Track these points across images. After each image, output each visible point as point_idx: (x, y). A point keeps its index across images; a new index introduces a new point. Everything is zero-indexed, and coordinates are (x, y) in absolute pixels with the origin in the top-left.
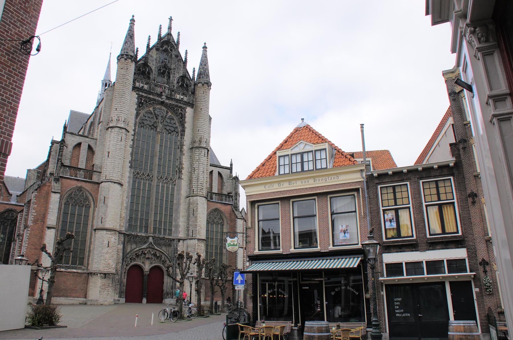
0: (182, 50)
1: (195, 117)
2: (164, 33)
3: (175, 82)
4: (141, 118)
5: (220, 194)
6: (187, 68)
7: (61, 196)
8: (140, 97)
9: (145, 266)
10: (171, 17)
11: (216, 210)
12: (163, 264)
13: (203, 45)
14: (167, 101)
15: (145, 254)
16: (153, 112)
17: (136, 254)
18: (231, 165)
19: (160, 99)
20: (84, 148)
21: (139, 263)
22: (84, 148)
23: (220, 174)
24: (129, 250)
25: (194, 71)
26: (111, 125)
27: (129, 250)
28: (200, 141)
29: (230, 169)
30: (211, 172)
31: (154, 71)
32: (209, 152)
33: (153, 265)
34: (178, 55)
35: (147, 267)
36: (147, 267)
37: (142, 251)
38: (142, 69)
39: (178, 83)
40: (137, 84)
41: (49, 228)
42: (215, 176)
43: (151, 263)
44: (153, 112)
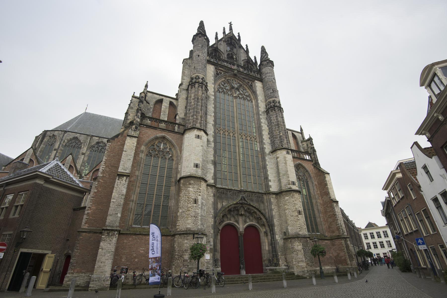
0: (243, 44)
1: (264, 88)
7: (138, 140)
9: (238, 224)
18: (301, 130)
21: (232, 221)
24: (219, 206)
25: (255, 58)
27: (219, 206)
29: (302, 133)
33: (247, 224)
34: (241, 47)
35: (241, 227)
36: (241, 227)
41: (121, 175)
43: (245, 222)
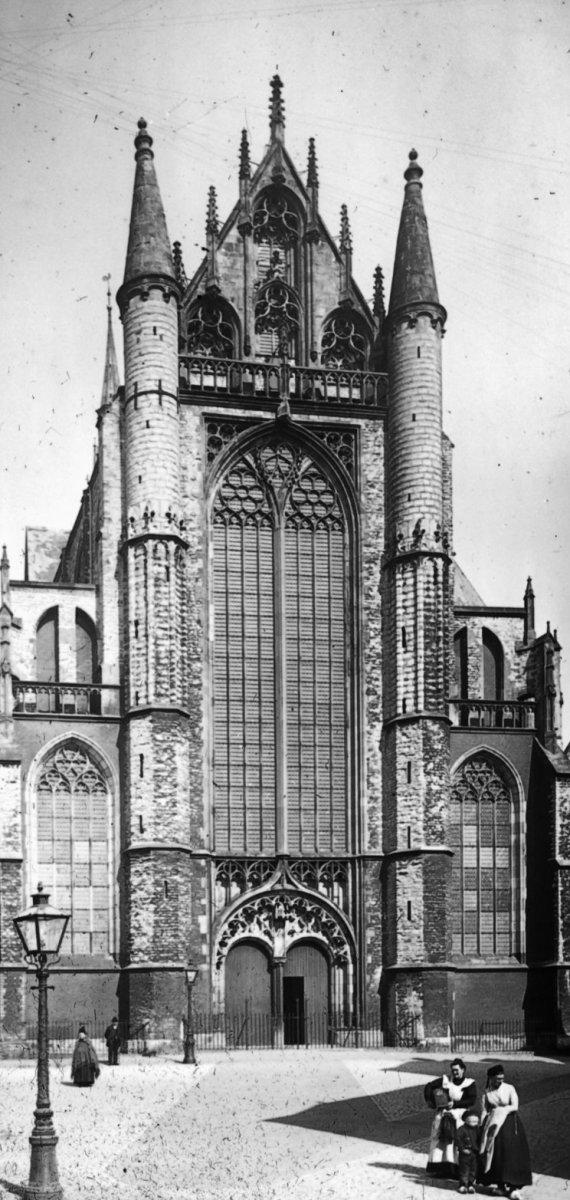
2: (257, 154)
3: (319, 339)
4: (219, 493)
5: (496, 704)
6: (356, 275)
8: (211, 422)
10: (276, 77)
11: (483, 756)
12: (324, 934)
13: (405, 164)
14: (295, 417)
15: (271, 909)
16: (254, 466)
17: (245, 911)
19: (269, 415)
20: (67, 622)
22: (67, 622)
23: (490, 637)
25: (379, 276)
26: (131, 533)
28: (418, 534)
30: (462, 635)
31: (241, 317)
32: (451, 567)
34: (320, 233)
37: (263, 902)
38: (207, 322)
39: (326, 341)
40: (195, 380)
42: (475, 641)
44: (254, 466)
